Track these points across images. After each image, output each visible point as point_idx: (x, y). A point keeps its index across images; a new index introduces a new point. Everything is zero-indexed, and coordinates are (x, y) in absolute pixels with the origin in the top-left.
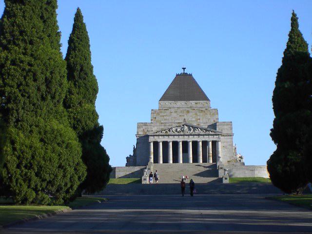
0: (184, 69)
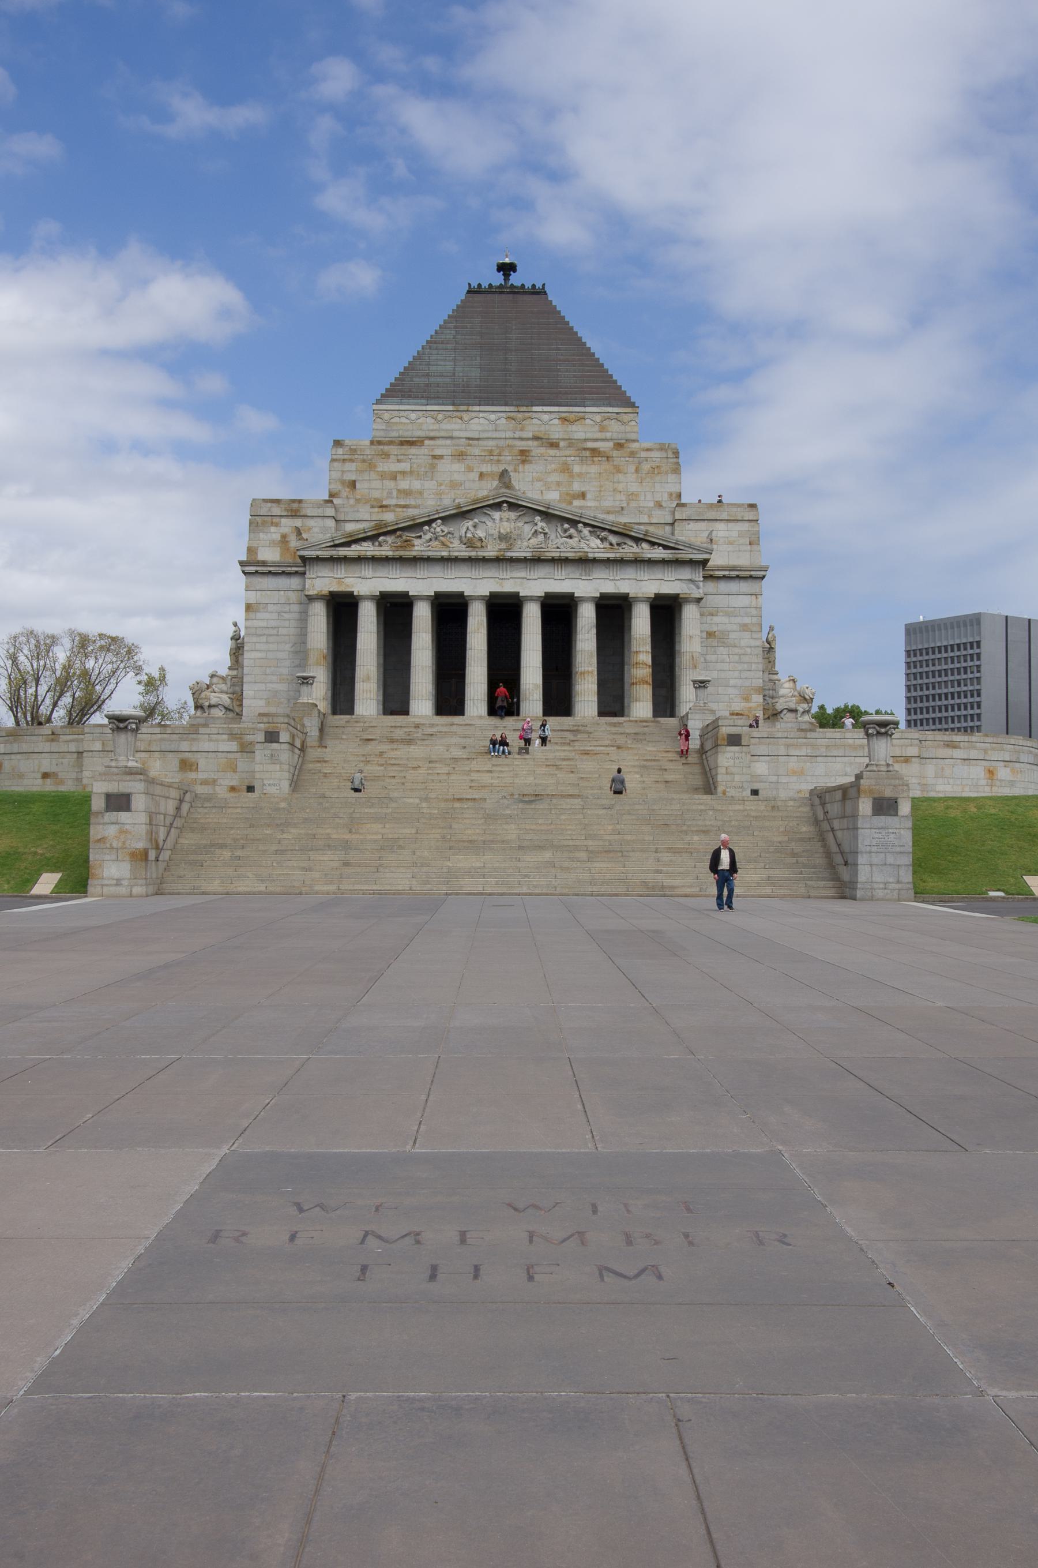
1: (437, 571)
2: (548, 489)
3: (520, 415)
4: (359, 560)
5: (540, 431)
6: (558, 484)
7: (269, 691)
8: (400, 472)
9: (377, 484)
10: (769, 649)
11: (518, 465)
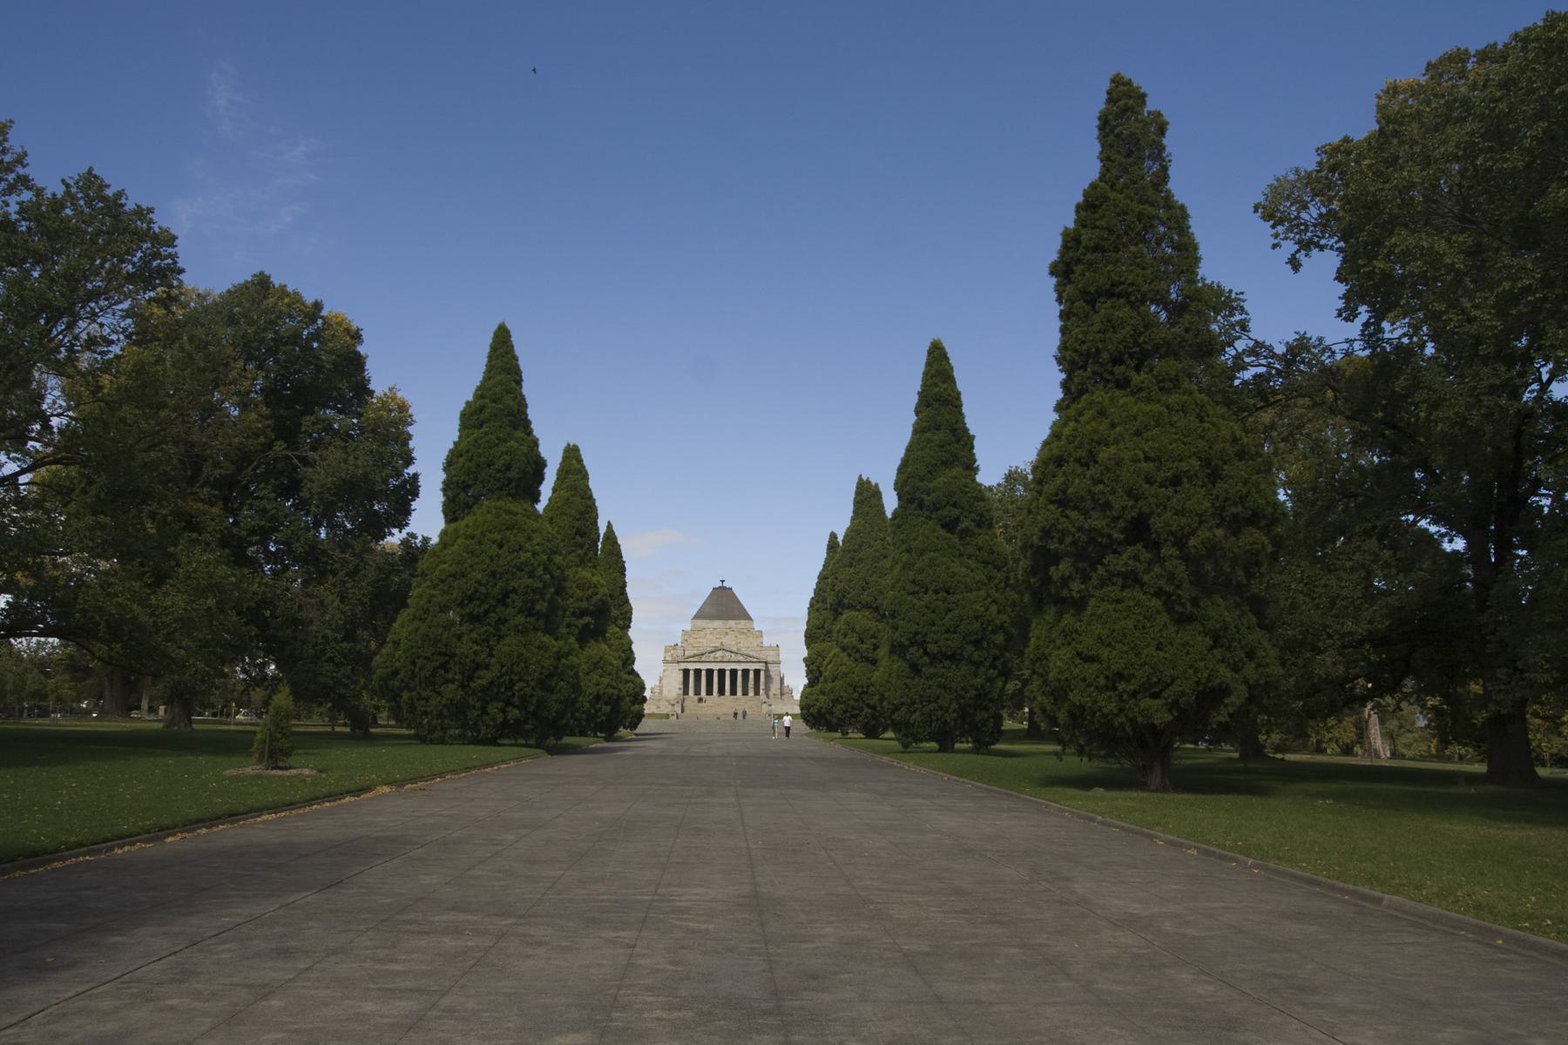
0: (722, 581)
10: (782, 680)
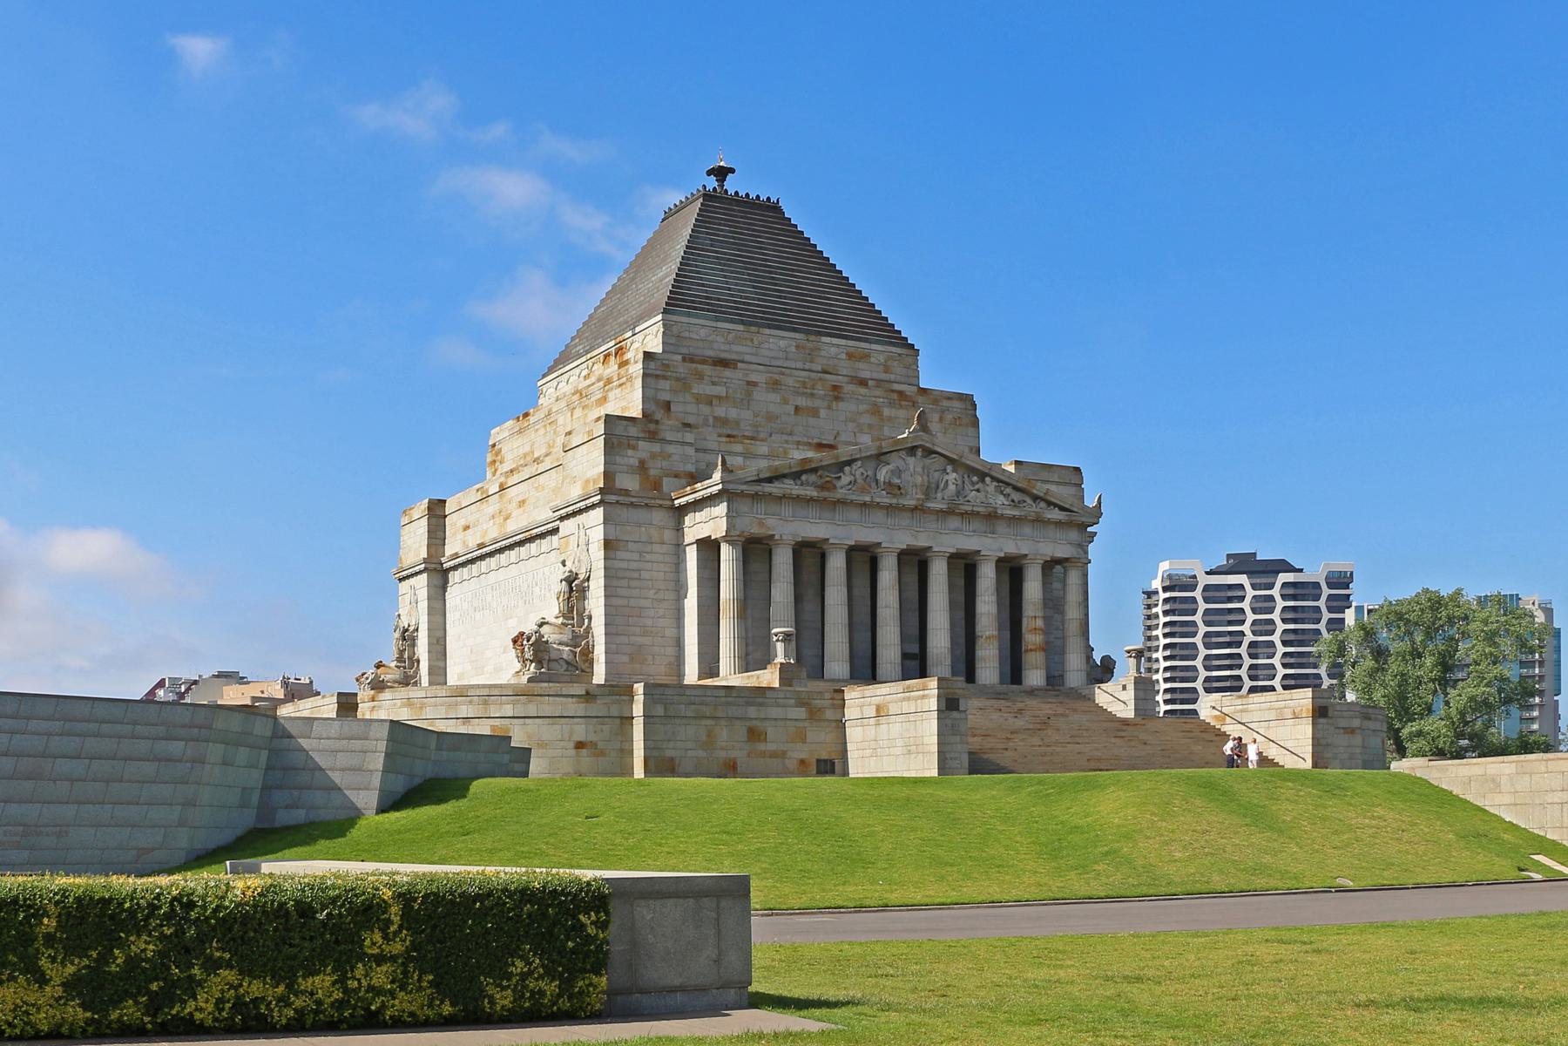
1: (854, 514)
2: (861, 431)
3: (809, 345)
4: (782, 499)
5: (829, 365)
6: (870, 426)
7: (633, 645)
8: (716, 396)
9: (692, 408)
11: (832, 402)
